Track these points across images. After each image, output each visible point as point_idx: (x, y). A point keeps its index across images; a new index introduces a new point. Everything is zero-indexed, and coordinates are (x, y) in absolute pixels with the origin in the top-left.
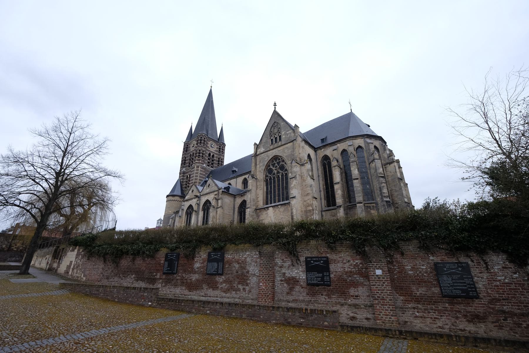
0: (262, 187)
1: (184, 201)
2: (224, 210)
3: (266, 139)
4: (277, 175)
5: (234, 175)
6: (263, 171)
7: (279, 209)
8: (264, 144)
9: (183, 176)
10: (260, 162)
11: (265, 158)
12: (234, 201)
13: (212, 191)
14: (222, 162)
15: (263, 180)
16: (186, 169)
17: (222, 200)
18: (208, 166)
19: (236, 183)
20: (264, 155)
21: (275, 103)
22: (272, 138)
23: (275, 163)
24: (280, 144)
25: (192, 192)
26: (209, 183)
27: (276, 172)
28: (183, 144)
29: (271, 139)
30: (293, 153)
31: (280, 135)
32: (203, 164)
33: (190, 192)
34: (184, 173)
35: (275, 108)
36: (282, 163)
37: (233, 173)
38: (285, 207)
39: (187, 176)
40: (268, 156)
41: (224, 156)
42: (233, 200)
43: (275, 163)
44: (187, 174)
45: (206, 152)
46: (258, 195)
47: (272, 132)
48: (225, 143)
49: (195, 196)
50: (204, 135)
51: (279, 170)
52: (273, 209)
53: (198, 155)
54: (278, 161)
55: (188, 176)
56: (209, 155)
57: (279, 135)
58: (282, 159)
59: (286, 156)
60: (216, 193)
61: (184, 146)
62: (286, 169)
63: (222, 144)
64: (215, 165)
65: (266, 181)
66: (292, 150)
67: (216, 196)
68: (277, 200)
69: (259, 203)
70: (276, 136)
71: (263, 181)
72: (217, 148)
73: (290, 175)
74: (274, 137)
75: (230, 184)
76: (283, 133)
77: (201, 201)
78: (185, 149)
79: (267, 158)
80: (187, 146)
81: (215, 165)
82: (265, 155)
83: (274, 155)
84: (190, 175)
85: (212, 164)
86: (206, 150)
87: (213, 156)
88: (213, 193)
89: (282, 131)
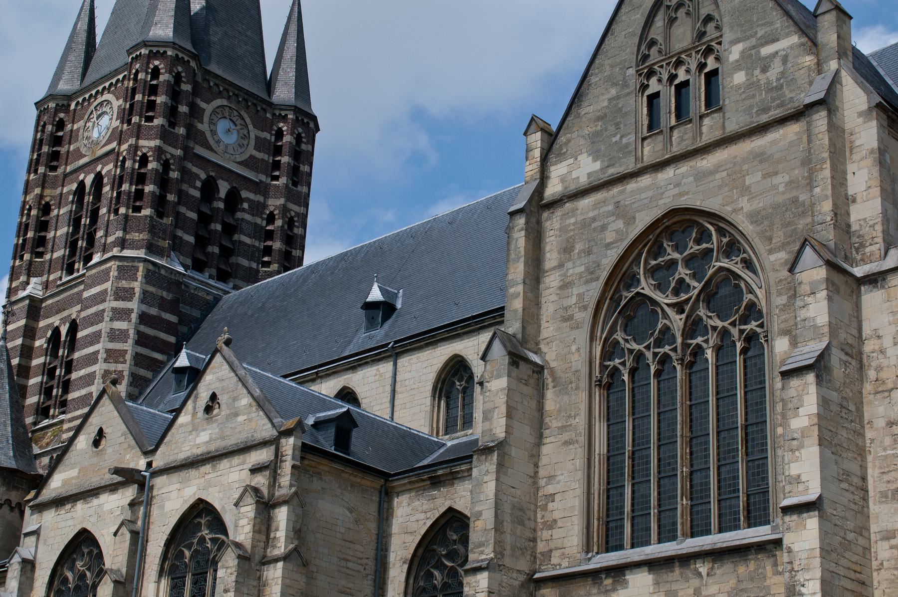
0: (580, 421)
1: (41, 508)
2: (310, 577)
3: (613, 92)
4: (685, 346)
5: (381, 335)
6: (585, 317)
7: (695, 582)
8: (599, 126)
10: (567, 249)
11: (604, 228)
12: (384, 516)
13: (233, 440)
15: (585, 371)
16: (46, 285)
17: (302, 505)
19: (394, 392)
20: (596, 206)
22: (654, 86)
23: (673, 263)
24: (710, 129)
25: (96, 443)
26: (216, 387)
27: (677, 321)
28: (33, 114)
29: (648, 92)
30: (803, 197)
31: (711, 64)
33: (83, 442)
36: (725, 263)
37: (371, 324)
38: (742, 569)
39: (56, 331)
40: (622, 212)
42: (373, 509)
43: (673, 263)
44: (55, 320)
45: (184, 171)
46: (551, 478)
47: (653, 43)
48: (316, 108)
49: (117, 471)
51: (702, 312)
52: (657, 583)
54: (693, 248)
55: (64, 330)
56: (209, 188)
57: (702, 66)
58: (721, 232)
59: (755, 217)
60: (263, 456)
61: (39, 126)
62: (752, 306)
64: (244, 262)
65: (609, 386)
66: (799, 172)
67: (261, 481)
68: (681, 521)
69: (557, 533)
70: (682, 76)
71: (584, 383)
72: (260, 144)
73: (781, 345)
74: (672, 77)
75: (347, 395)
76: (734, 53)
77: (155, 511)
78: (45, 149)
79: (620, 224)
80: (61, 125)
81: (244, 262)
82: (604, 202)
83: (667, 202)
84: (74, 327)
85: (227, 253)
86: (189, 154)
87: (233, 199)
88: (236, 460)
89: (728, 36)
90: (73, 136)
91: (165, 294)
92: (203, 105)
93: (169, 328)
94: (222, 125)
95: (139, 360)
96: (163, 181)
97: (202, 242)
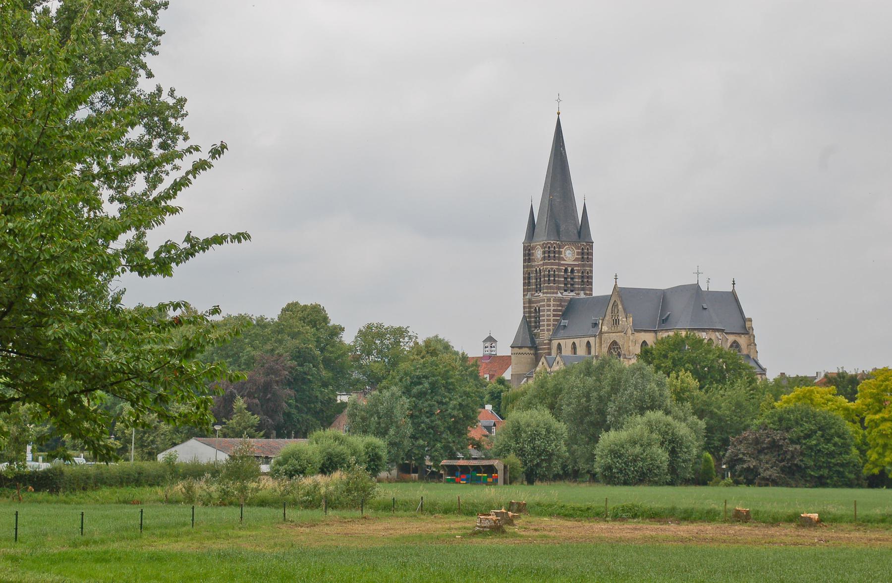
9: (530, 307)
14: (588, 277)
16: (532, 295)
18: (565, 291)
21: (616, 276)
32: (557, 293)
35: (616, 282)
39: (536, 308)
41: (591, 266)
44: (535, 305)
45: (559, 270)
50: (552, 242)
53: (547, 279)
56: (566, 271)
63: (585, 244)
64: (577, 286)
72: (578, 254)
81: (577, 286)
85: (572, 285)
87: (572, 271)
91: (558, 303)
92: (561, 250)
93: (560, 311)
94: (568, 252)
96: (554, 276)
97: (565, 284)
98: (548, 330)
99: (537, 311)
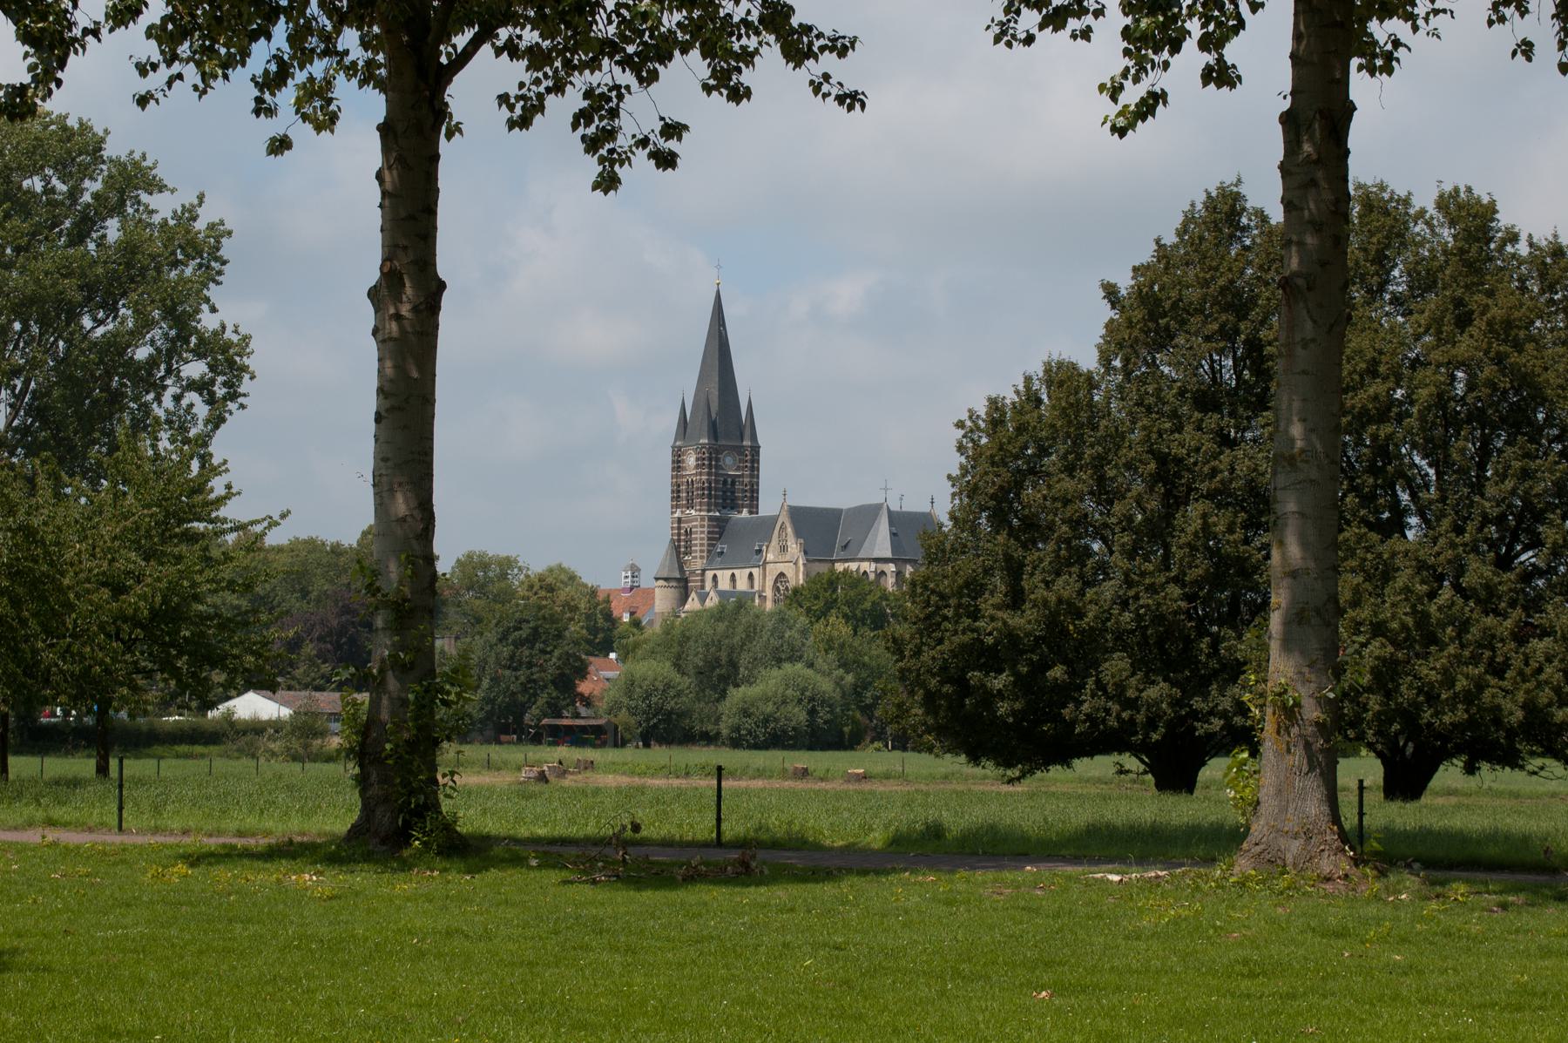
34: (679, 520)
56: (725, 482)
90: (683, 461)
95: (709, 545)
97: (724, 500)
98: (702, 557)
99: (688, 533)
